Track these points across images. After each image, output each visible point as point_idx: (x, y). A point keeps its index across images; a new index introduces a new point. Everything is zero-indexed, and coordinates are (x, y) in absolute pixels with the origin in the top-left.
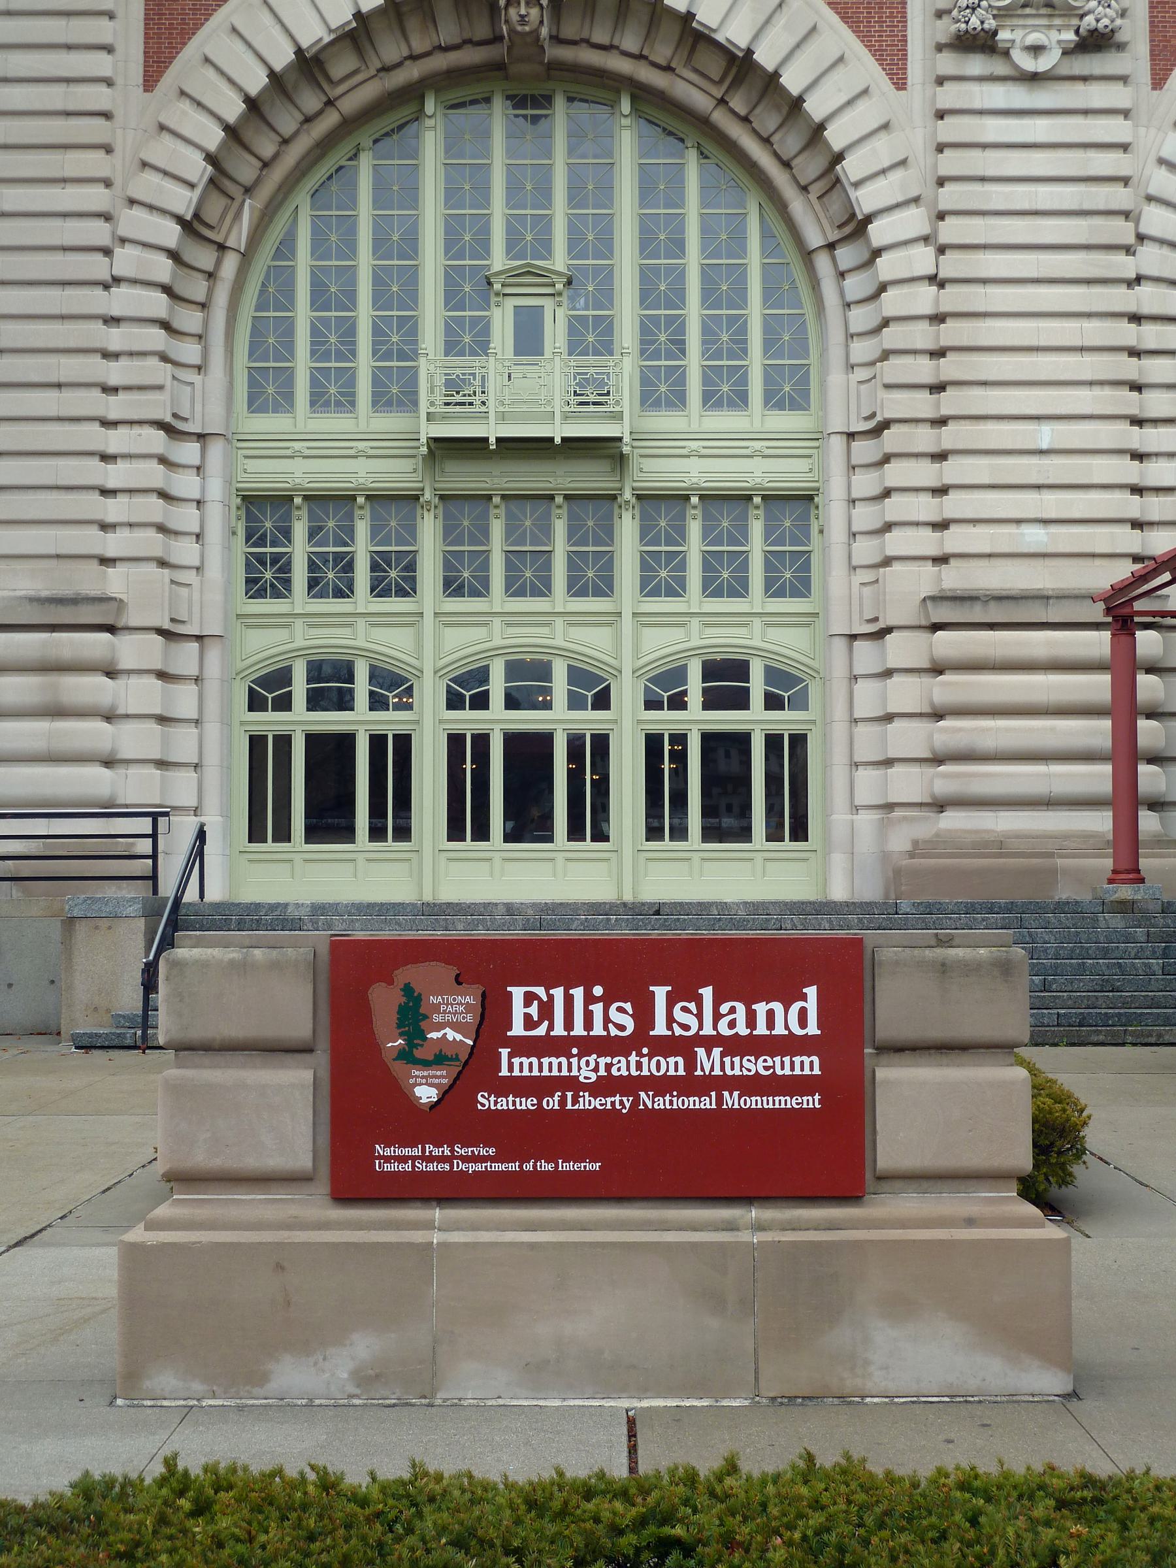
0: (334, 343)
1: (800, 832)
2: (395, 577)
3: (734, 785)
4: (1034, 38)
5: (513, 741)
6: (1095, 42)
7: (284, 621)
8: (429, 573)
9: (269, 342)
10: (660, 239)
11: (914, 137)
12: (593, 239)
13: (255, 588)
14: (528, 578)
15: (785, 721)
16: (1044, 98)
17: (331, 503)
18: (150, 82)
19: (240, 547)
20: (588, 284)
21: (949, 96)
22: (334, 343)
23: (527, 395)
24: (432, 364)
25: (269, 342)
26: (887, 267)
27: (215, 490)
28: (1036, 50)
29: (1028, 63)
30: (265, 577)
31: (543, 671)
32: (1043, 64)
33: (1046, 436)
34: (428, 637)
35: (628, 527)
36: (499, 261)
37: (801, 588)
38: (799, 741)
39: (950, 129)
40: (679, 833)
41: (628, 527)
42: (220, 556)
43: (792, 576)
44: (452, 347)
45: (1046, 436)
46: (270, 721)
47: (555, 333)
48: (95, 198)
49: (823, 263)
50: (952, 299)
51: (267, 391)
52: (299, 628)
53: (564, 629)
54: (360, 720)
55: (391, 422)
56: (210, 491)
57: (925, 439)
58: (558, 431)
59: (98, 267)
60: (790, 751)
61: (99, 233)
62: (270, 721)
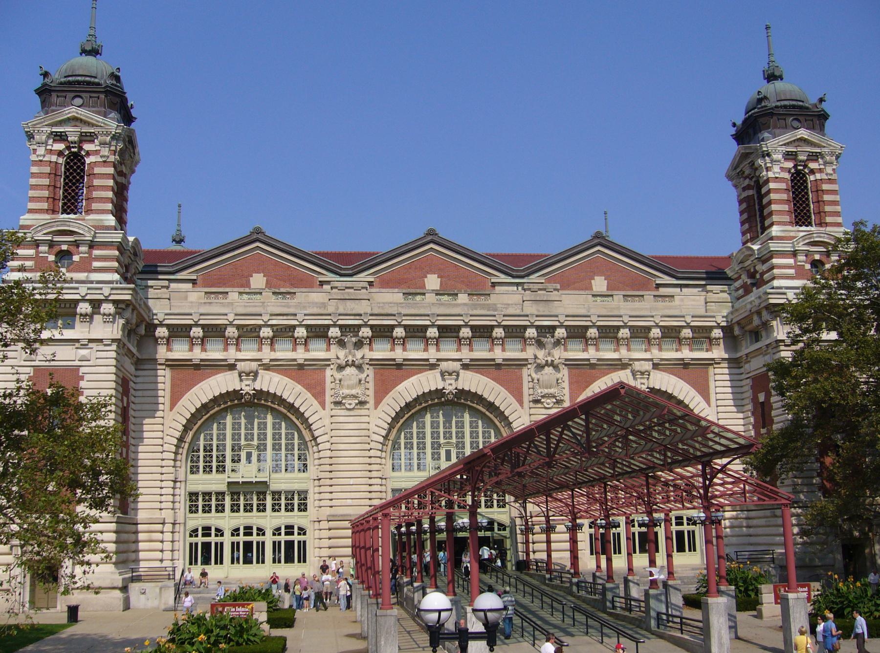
0: (208, 459)
1: (305, 561)
2: (220, 509)
3: (292, 552)
4: (350, 402)
5: (245, 543)
6: (362, 403)
7: (197, 518)
8: (228, 507)
9: (195, 460)
10: (276, 437)
11: (327, 421)
12: (263, 437)
13: (191, 512)
14: (248, 508)
15: (302, 538)
16: (352, 413)
17: (207, 495)
18: (171, 409)
19: (188, 503)
20: (262, 448)
21: (334, 412)
22: (208, 459)
23: (247, 472)
24: (228, 463)
25: (195, 460)
26: (321, 447)
27: (183, 493)
28: (350, 404)
29: (348, 407)
30: (193, 509)
31: (251, 528)
32: (351, 407)
33: (352, 481)
34: (227, 521)
35: (269, 498)
36: (243, 442)
37: (305, 510)
38: (305, 542)
39: (335, 419)
40: (280, 562)
41: (269, 498)
42: (183, 504)
43: (303, 508)
44: (233, 461)
45: (352, 481)
46: (194, 540)
47: (254, 458)
48: (160, 434)
49: (309, 444)
50: (334, 454)
51: (194, 470)
52: (199, 520)
53: (255, 519)
54: (213, 539)
55: (220, 476)
56: (181, 492)
57: (328, 482)
58: (254, 480)
59: (160, 449)
60: (303, 545)
61: (160, 442)
62: (194, 540)
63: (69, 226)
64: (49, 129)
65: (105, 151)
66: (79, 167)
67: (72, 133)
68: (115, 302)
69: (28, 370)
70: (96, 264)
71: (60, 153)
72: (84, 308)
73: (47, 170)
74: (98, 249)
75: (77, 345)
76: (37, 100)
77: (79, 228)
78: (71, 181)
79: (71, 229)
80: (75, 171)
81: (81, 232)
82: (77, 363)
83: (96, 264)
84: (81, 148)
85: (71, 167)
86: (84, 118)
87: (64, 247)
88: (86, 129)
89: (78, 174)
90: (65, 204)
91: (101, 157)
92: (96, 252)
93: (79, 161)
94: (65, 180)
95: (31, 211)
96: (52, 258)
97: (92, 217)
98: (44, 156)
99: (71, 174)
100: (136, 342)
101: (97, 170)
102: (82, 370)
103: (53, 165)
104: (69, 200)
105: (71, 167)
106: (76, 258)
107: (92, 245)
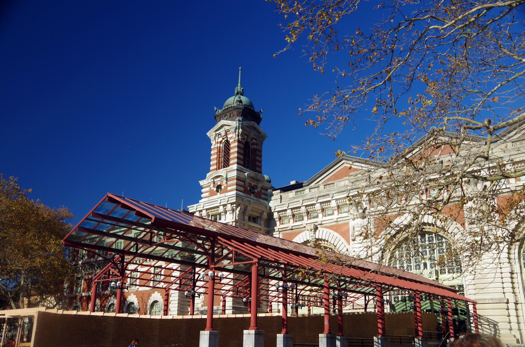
64: (214, 133)
67: (222, 132)
68: (232, 204)
70: (229, 188)
71: (221, 142)
83: (229, 188)
87: (219, 184)
96: (215, 189)
106: (223, 187)
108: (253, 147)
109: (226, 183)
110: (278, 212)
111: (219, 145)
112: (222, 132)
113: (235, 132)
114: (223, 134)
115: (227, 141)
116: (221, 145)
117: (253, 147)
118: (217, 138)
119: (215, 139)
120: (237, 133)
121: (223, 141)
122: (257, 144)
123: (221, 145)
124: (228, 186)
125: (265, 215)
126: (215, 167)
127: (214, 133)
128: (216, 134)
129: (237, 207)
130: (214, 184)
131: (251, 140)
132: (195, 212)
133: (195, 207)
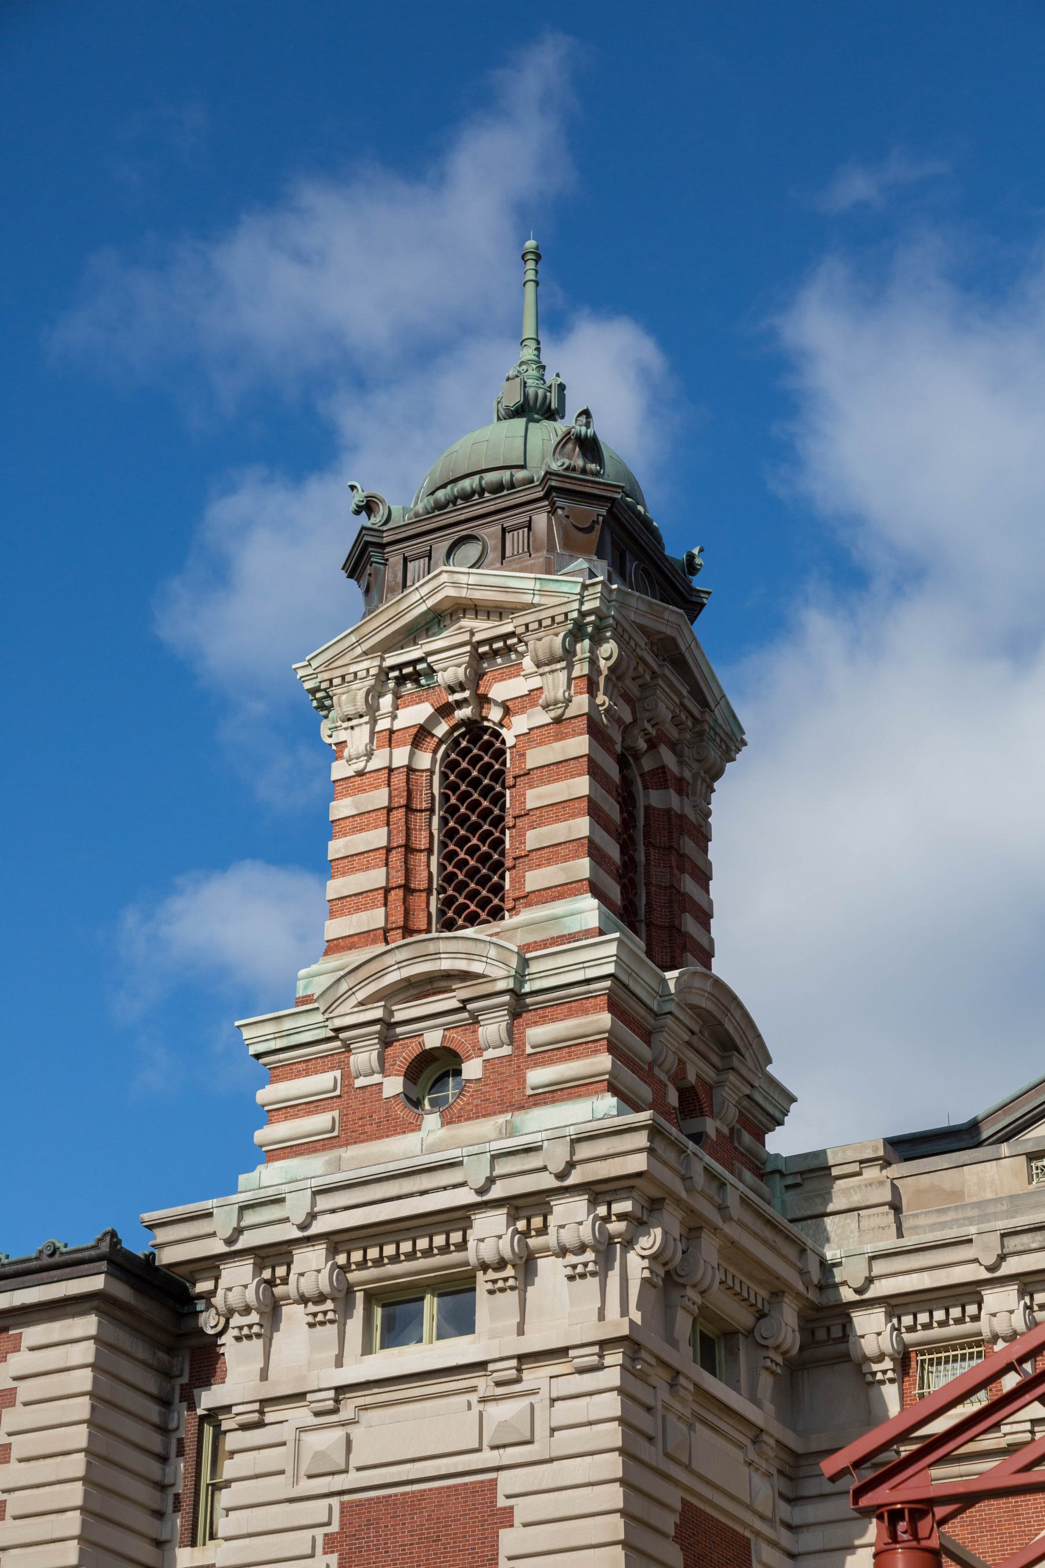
63: (436, 955)
64: (372, 664)
65: (555, 684)
66: (486, 769)
67: (447, 655)
68: (598, 1192)
69: (317, 1511)
70: (538, 1076)
71: (421, 735)
72: (491, 1234)
73: (380, 797)
74: (544, 1020)
75: (483, 1384)
76: (353, 589)
77: (469, 956)
78: (463, 820)
79: (446, 965)
80: (475, 783)
81: (477, 967)
82: (489, 1458)
83: (538, 1076)
84: (483, 700)
85: (464, 775)
86: (477, 595)
87: (433, 1039)
88: (484, 628)
89: (486, 792)
90: (449, 902)
91: (546, 707)
92: (537, 1034)
93: (487, 747)
94: (444, 821)
95: (335, 946)
96: (394, 1085)
97: (526, 915)
98: (369, 755)
99: (464, 797)
100: (766, 1381)
101: (535, 757)
102: (507, 1482)
103: (399, 780)
104: (461, 887)
105: (464, 775)
106: (472, 1069)
107: (519, 1006)
108: (656, 798)
109: (512, 1037)
110: (895, 1305)
111: (401, 756)
112: (447, 655)
113: (569, 654)
114: (451, 671)
115: (474, 728)
116: (424, 760)
117: (656, 798)
118: (386, 702)
119: (372, 710)
120: (581, 669)
121: (441, 729)
122: (681, 787)
123: (424, 760)
124: (523, 1058)
125: (787, 1327)
126: (375, 918)
127: (372, 664)
128: (384, 673)
129: (638, 1223)
130: (386, 1042)
131: (652, 745)
132: (211, 1265)
133: (224, 1221)
